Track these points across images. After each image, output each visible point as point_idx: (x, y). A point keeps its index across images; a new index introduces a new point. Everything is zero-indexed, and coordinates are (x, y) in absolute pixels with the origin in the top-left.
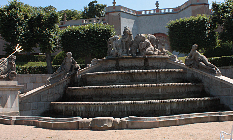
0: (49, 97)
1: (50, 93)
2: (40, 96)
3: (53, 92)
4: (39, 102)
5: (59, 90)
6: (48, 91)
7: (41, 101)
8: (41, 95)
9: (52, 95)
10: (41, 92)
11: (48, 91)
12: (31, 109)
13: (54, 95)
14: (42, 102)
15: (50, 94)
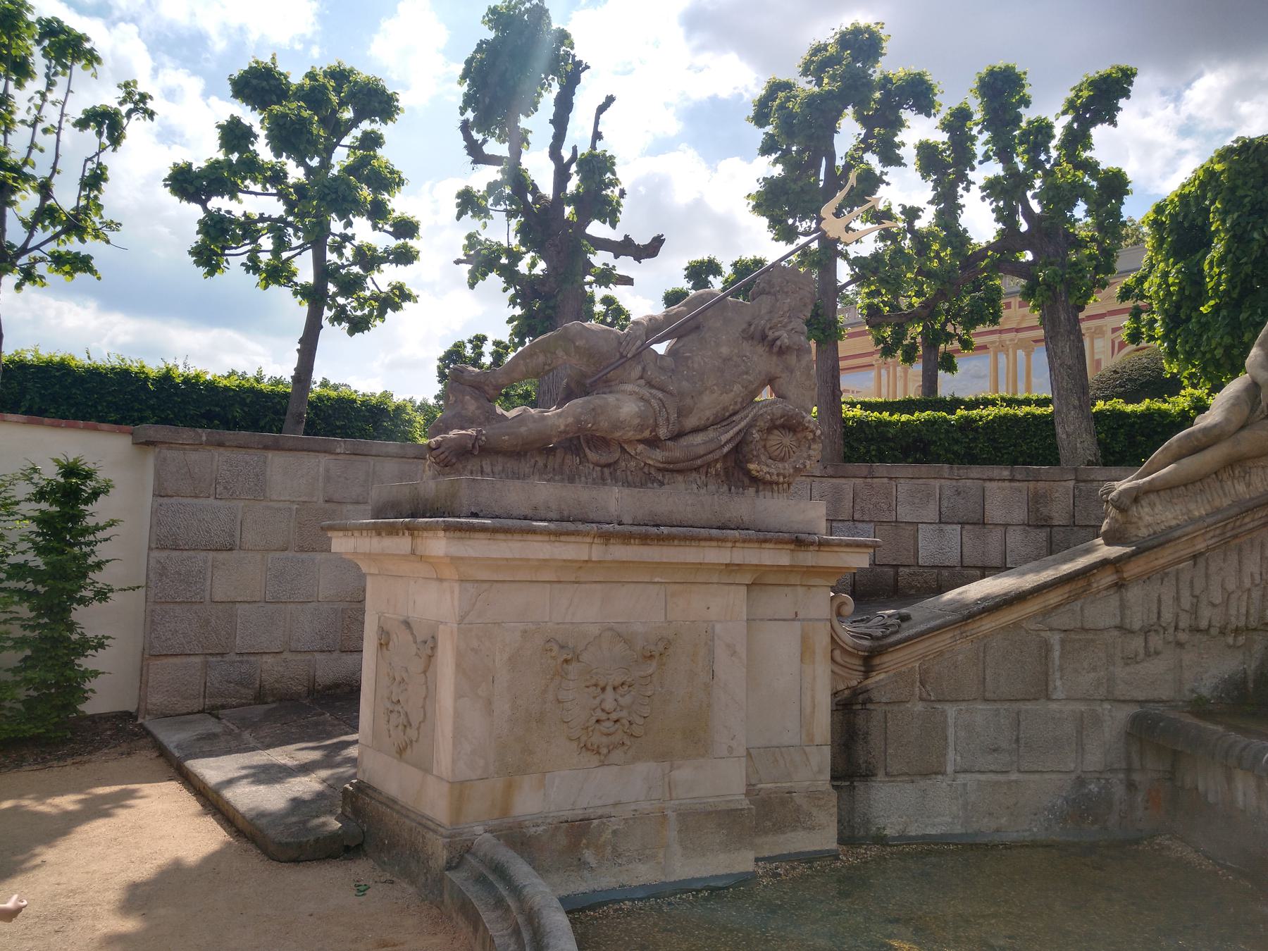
0: (1130, 660)
1: (1137, 625)
2: (1046, 647)
3: (1167, 616)
4: (1029, 706)
5: (1227, 602)
6: (1123, 606)
7: (1043, 691)
8: (1055, 639)
9: (1156, 641)
10: (1047, 612)
11: (1123, 606)
12: (950, 769)
13: (1180, 645)
14: (1054, 706)
15: (1146, 631)
